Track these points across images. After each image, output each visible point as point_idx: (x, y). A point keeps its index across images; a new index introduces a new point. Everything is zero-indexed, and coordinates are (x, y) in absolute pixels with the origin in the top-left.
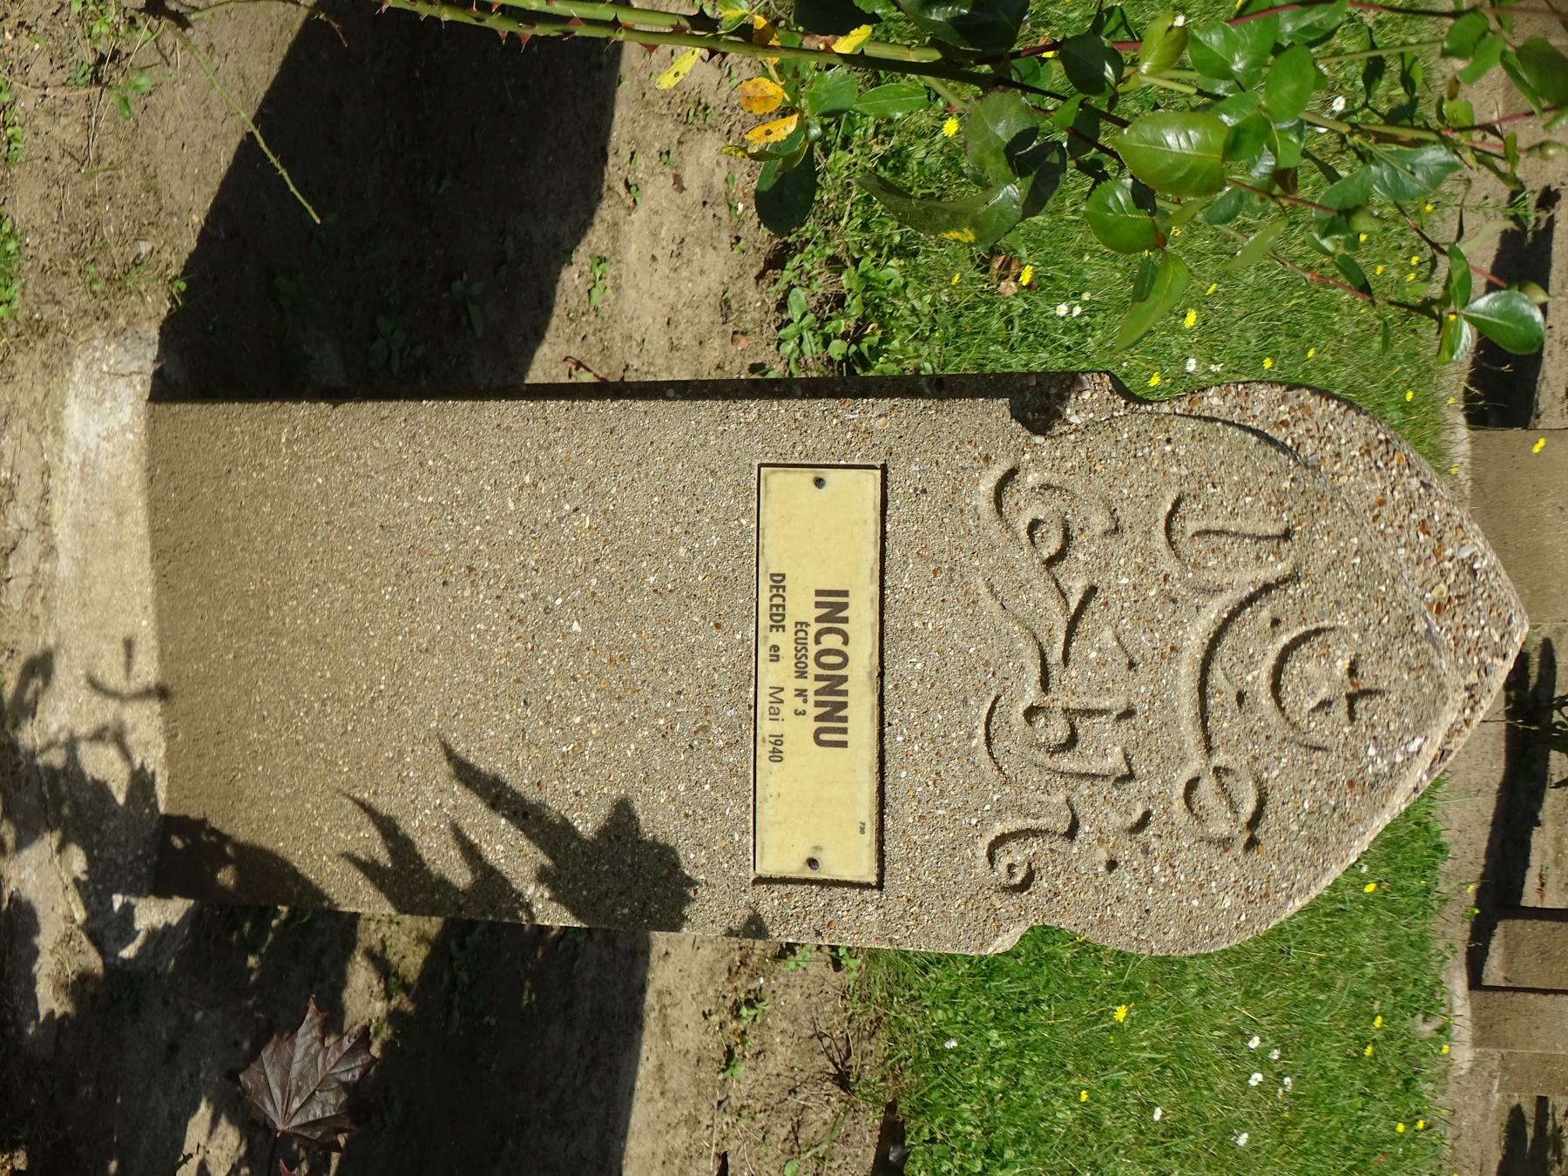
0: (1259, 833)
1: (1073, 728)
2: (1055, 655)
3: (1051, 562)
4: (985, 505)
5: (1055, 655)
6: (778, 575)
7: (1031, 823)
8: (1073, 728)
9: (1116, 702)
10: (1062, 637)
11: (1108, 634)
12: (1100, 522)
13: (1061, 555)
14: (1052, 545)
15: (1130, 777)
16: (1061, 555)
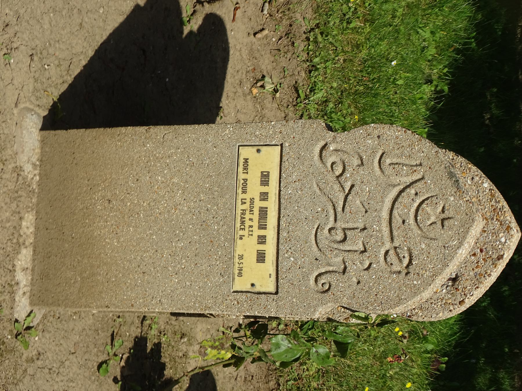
0: (411, 269)
1: (345, 234)
2: (339, 209)
3: (338, 177)
4: (316, 157)
5: (339, 209)
6: (245, 179)
7: (331, 269)
8: (345, 234)
9: (361, 226)
10: (341, 203)
11: (358, 202)
12: (356, 162)
13: (341, 175)
14: (339, 170)
15: (365, 251)
16: (341, 175)
